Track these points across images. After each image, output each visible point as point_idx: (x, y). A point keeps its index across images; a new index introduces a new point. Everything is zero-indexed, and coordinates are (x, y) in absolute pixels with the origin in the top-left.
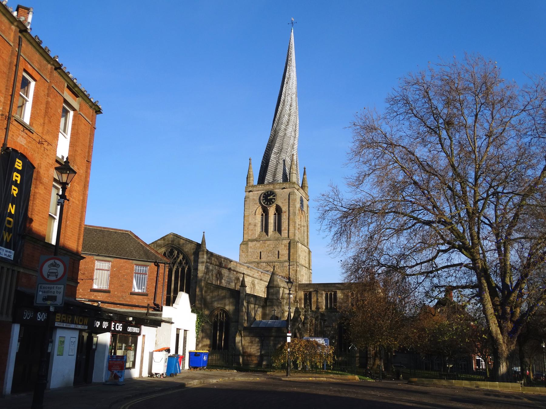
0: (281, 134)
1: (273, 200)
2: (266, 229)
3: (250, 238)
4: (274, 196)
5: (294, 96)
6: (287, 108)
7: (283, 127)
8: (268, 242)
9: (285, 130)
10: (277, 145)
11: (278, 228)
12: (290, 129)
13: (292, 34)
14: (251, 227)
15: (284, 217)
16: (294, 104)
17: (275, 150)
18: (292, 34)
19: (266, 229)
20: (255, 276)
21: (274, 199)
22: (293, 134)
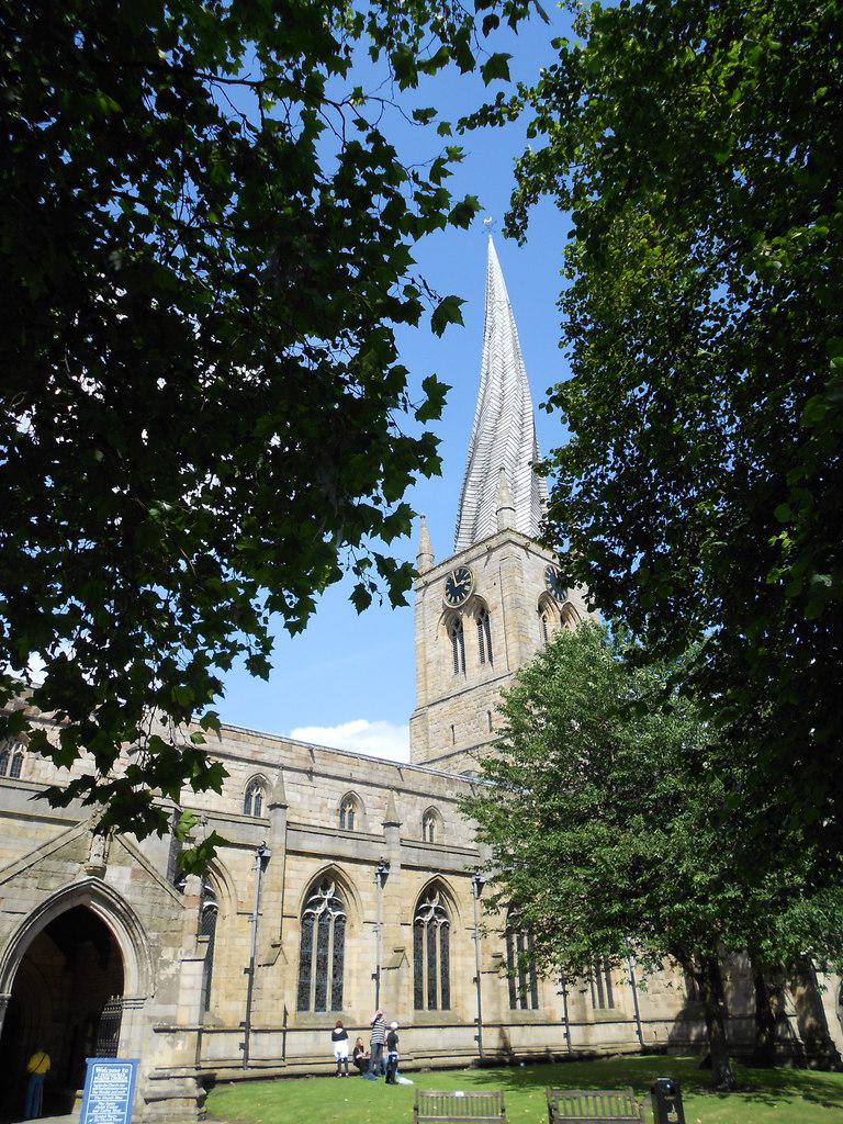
0: (485, 440)
1: (467, 588)
2: (460, 664)
3: (430, 697)
4: (468, 577)
5: (510, 358)
6: (495, 383)
7: (489, 424)
8: (466, 697)
9: (494, 429)
10: (477, 466)
11: (487, 654)
12: (508, 424)
13: (491, 245)
14: (431, 669)
15: (495, 620)
16: (512, 374)
17: (474, 478)
18: (491, 245)
19: (460, 664)
20: (265, 758)
21: (469, 584)
22: (516, 432)
